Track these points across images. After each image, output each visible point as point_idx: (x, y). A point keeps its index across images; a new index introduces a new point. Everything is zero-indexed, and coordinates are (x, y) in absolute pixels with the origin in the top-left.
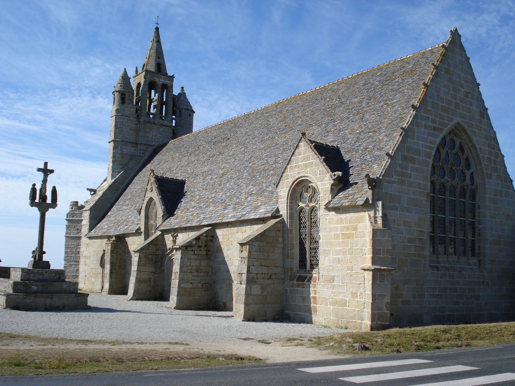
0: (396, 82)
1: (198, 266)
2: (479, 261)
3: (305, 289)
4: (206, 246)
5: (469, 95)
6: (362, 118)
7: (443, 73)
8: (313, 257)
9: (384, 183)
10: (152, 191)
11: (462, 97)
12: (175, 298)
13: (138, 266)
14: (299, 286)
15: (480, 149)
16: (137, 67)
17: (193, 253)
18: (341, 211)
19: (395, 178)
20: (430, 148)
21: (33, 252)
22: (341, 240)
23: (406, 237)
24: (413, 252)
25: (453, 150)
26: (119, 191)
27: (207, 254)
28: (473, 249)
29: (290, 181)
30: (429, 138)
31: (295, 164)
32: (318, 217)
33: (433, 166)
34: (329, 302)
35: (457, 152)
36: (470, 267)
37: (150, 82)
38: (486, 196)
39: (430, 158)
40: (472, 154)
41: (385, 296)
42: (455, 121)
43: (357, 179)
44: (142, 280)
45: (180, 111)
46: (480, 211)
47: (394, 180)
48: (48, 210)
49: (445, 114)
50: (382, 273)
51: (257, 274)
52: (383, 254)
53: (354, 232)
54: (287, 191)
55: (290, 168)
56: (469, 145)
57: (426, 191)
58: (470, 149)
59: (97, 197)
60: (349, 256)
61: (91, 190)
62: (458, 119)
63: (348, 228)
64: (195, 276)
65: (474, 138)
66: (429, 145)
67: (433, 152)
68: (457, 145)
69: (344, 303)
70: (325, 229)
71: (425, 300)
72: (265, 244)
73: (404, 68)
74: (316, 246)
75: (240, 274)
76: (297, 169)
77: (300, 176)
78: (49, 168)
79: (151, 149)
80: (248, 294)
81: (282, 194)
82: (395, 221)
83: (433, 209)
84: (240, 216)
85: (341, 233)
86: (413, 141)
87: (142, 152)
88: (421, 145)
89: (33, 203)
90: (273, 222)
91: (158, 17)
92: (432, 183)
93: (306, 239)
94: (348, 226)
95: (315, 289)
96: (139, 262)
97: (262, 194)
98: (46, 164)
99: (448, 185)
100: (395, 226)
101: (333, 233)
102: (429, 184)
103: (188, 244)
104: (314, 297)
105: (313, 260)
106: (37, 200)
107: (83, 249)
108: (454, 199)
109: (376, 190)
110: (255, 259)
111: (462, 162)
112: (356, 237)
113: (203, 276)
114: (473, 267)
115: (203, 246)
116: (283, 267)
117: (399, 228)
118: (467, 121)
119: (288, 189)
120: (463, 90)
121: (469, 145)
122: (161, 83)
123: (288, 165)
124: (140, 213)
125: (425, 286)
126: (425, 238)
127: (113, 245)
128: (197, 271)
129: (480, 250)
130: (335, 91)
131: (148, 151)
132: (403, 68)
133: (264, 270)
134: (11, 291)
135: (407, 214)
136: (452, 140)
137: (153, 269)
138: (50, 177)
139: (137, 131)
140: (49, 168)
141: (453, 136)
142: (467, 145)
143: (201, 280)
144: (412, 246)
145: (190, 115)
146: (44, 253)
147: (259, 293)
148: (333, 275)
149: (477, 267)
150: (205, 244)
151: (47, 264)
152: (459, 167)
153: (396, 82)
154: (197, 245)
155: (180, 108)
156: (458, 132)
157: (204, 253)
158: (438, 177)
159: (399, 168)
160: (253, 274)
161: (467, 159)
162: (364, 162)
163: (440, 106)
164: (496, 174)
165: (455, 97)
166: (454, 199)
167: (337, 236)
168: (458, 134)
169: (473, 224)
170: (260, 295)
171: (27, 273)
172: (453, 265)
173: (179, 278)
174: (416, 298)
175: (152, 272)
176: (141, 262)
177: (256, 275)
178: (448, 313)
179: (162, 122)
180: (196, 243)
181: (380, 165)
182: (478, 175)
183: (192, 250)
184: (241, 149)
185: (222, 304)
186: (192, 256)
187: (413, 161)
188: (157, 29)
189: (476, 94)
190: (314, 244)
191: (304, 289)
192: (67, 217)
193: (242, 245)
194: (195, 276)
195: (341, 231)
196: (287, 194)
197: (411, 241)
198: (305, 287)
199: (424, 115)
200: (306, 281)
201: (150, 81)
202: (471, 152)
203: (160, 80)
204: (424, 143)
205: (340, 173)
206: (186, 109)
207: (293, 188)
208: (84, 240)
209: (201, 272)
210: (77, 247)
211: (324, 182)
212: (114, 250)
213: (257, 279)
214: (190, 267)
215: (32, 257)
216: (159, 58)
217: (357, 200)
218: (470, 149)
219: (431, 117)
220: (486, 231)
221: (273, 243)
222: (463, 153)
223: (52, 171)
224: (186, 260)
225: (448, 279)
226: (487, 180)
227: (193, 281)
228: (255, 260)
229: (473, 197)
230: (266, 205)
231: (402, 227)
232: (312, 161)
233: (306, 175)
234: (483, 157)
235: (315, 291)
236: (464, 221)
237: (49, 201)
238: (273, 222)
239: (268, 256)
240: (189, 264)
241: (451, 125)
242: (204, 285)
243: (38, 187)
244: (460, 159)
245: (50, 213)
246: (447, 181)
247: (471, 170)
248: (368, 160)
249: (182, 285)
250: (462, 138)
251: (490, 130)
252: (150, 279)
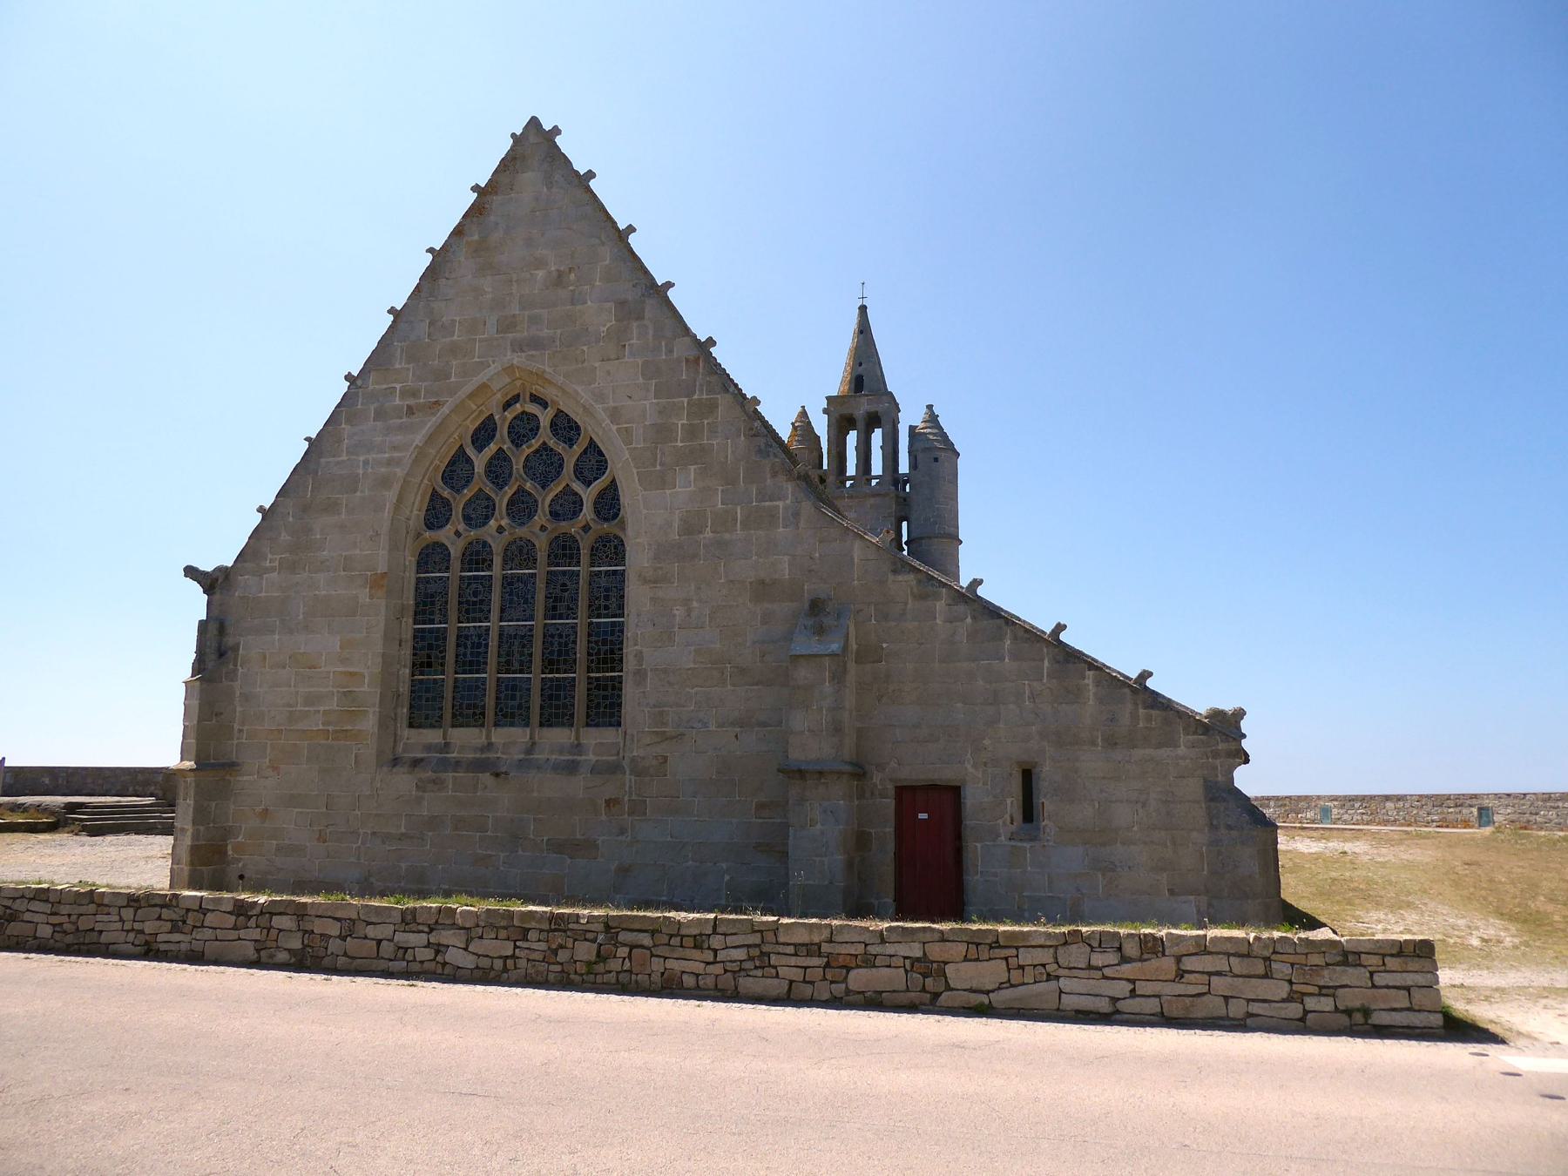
23: (297, 692)
24: (321, 727)
126: (366, 688)
187: (331, 507)
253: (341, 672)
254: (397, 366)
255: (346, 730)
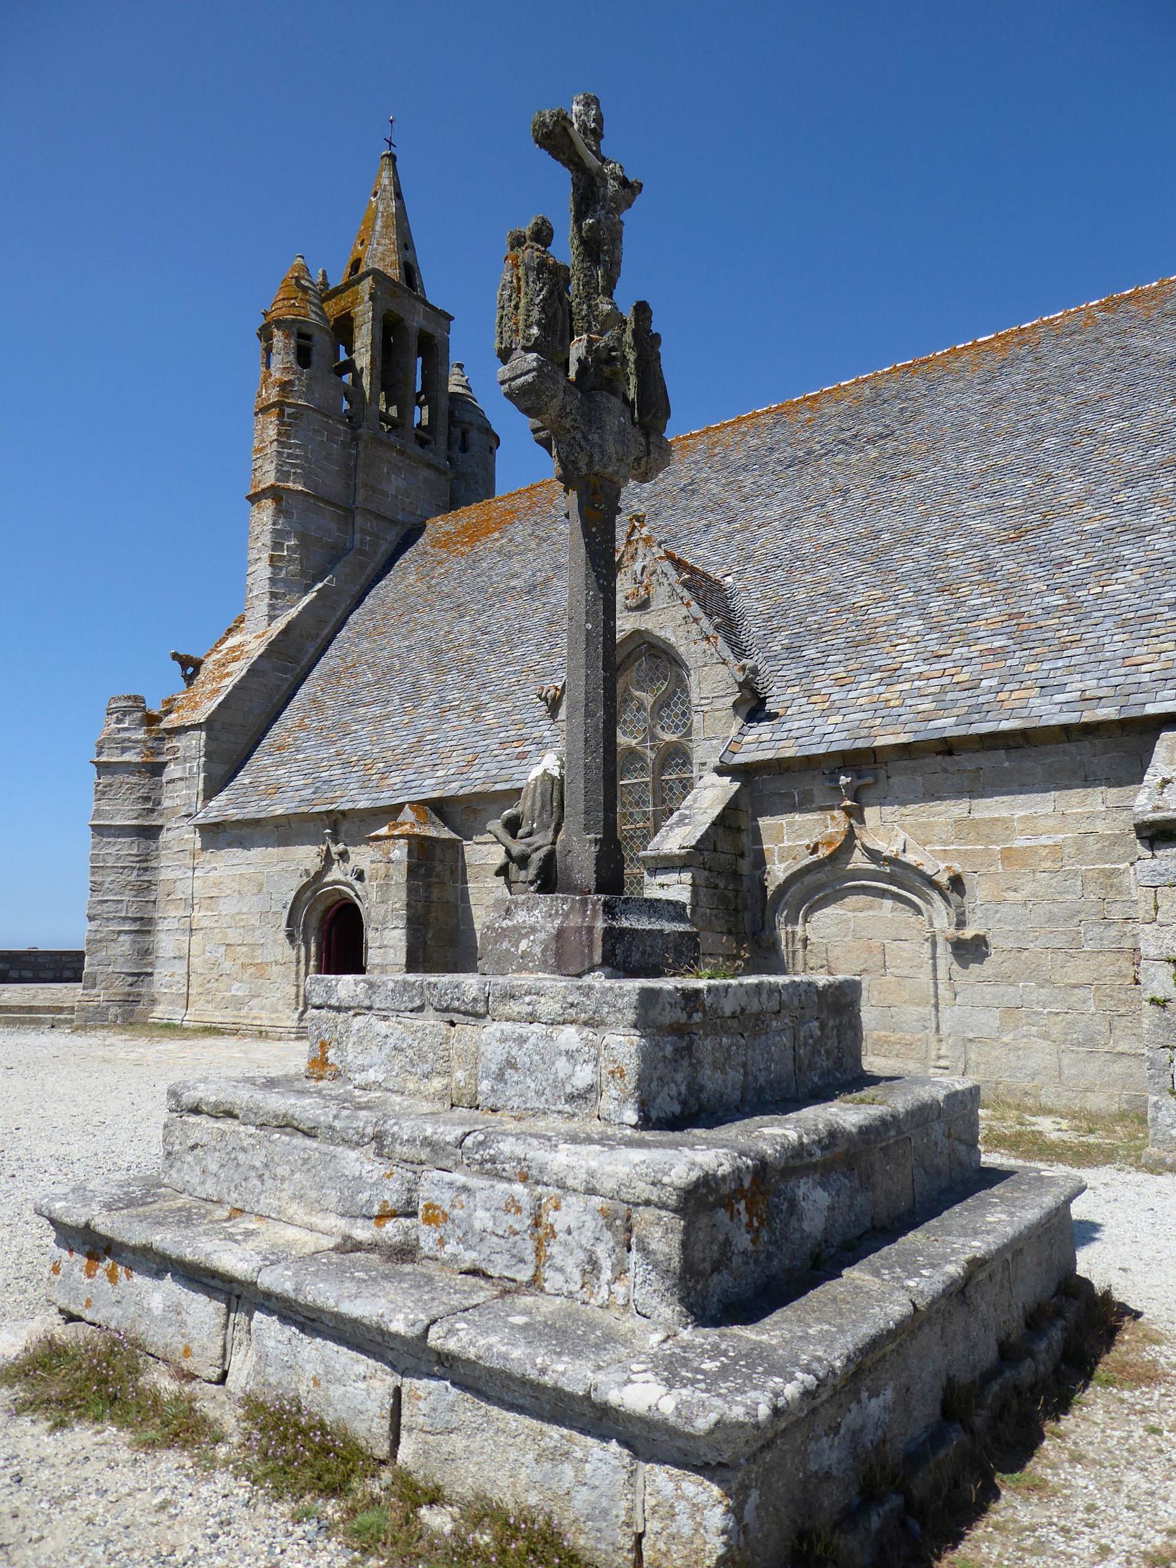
45: (464, 434)
79: (392, 536)
127: (414, 842)
139: (350, 471)
210: (145, 865)
212: (419, 866)
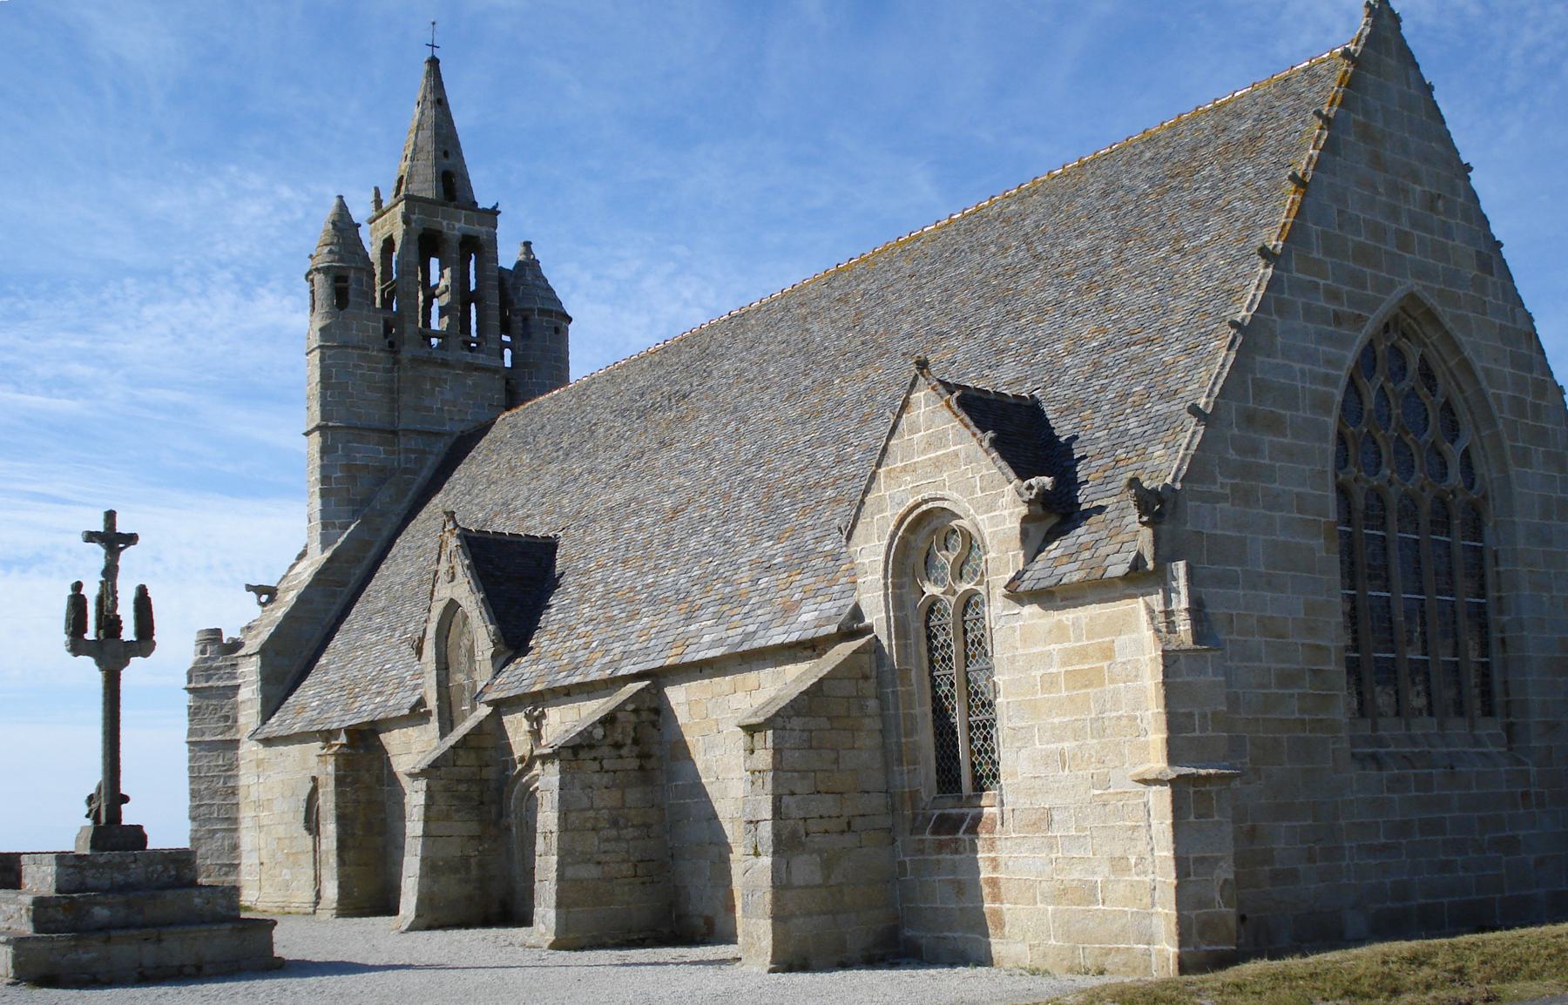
0: (1205, 179)
1: (615, 808)
2: (1509, 728)
3: (963, 856)
4: (636, 742)
5: (1440, 203)
6: (1104, 301)
7: (1352, 139)
8: (979, 752)
9: (1189, 503)
10: (452, 581)
11: (1418, 210)
12: (551, 915)
13: (427, 821)
14: (941, 847)
15: (1486, 371)
16: (377, 190)
17: (596, 766)
18: (1059, 599)
19: (1221, 484)
20: (1327, 380)
21: (90, 799)
22: (1064, 694)
23: (1269, 669)
24: (1297, 715)
25: (1400, 381)
26: (350, 586)
27: (641, 768)
28: (1487, 693)
29: (891, 515)
30: (1321, 348)
31: (902, 461)
32: (987, 626)
33: (1341, 439)
34: (1042, 894)
35: (1413, 389)
36: (1480, 750)
37: (421, 231)
38: (1517, 519)
39: (1328, 412)
40: (1462, 391)
41: (1217, 860)
42: (1399, 292)
43: (1102, 495)
44: (441, 863)
45: (525, 319)
46: (1501, 569)
47: (1220, 491)
48: (127, 663)
49: (1369, 271)
50: (1203, 789)
51: (805, 819)
52: (1203, 729)
53: (1105, 664)
54: (883, 550)
55: (885, 477)
56: (1452, 363)
57: (1323, 520)
58: (1453, 376)
59: (279, 612)
60: (1095, 741)
61: (259, 590)
62: (1408, 284)
63: (1083, 654)
64: (607, 840)
65: (1464, 339)
66: (1323, 370)
67: (1338, 395)
68: (1413, 364)
69: (1088, 893)
70: (1012, 660)
71: (1344, 864)
72: (823, 722)
73: (1226, 133)
74: (987, 716)
75: (751, 822)
76: (909, 478)
77: (919, 498)
78: (122, 527)
79: (441, 447)
80: (781, 885)
81: (867, 561)
82: (1232, 621)
83: (1350, 574)
84: (738, 639)
85: (1063, 670)
86: (1272, 360)
87: (413, 456)
88: (1299, 375)
89: (77, 645)
90: (844, 649)
91: (434, 23)
92: (1342, 491)
93: (953, 696)
94: (1084, 648)
95: (992, 855)
96: (427, 807)
97: (805, 565)
98: (110, 516)
99: (1393, 496)
100: (1232, 637)
101: (1039, 673)
102: (1332, 495)
103: (578, 741)
104: (992, 878)
105: (980, 764)
106: (90, 635)
107: (247, 778)
108: (1415, 537)
109: (1165, 527)
110: (795, 771)
111: (1431, 418)
112: (1112, 681)
113: (634, 839)
114: (1491, 749)
115: (629, 741)
116: (887, 792)
117: (1245, 641)
118: (1437, 287)
119: (886, 542)
120: (1418, 188)
121: (1452, 363)
122: (456, 232)
123: (879, 465)
124: (419, 651)
125: (1342, 822)
126: (1332, 667)
127: (340, 759)
128: (615, 823)
129: (1507, 694)
130: (1014, 220)
131: (431, 453)
132: (1223, 131)
133: (827, 805)
134: (27, 929)
135: (1269, 595)
136: (1397, 352)
137: (474, 827)
138: (127, 557)
139: (392, 394)
140: (122, 527)
141: (1399, 339)
142: (1445, 362)
143: (628, 852)
144: (1292, 696)
145: (557, 330)
146: (126, 799)
147: (818, 879)
148: (1047, 806)
149: (1505, 749)
150: (632, 734)
151: (137, 836)
152: (1422, 435)
153: (1205, 179)
154: (609, 740)
155: (523, 310)
156: (1412, 322)
157: (634, 764)
158: (1359, 471)
159: (1231, 451)
160: (792, 822)
161: (1448, 408)
162: (1119, 440)
163: (1350, 244)
164: (1541, 449)
165: (1394, 213)
166: (1415, 537)
167: (1050, 682)
168: (1415, 331)
169: (1479, 613)
170: (819, 886)
171: (74, 866)
172: (1427, 749)
173: (559, 848)
174: (1314, 862)
175: (472, 837)
176: (434, 809)
177: (801, 823)
178: (1422, 901)
179: (469, 357)
180: (605, 736)
181: (1170, 445)
182: (1485, 456)
183: (595, 759)
184: (726, 425)
185: (700, 922)
186: (596, 777)
187: (1274, 424)
188: (434, 63)
189: (1461, 200)
190: (980, 712)
191: (957, 857)
192: (190, 681)
193: (751, 730)
194: (607, 840)
195: (1064, 664)
196: (882, 558)
197: (1287, 679)
198: (961, 849)
199: (1301, 276)
200: (962, 831)
201: (424, 229)
202: (1458, 384)
203: (455, 226)
204: (1307, 367)
205: (1047, 481)
206: (542, 312)
207: (902, 538)
208: (249, 750)
209: (626, 827)
210: (229, 773)
211: (997, 513)
212: (345, 776)
213: (807, 834)
214: (591, 813)
215: (87, 816)
216: (446, 154)
217: (1106, 563)
218: (1453, 376)
219: (1322, 282)
220: (1525, 633)
221: (848, 716)
222: (1432, 389)
223: (131, 539)
224: (577, 791)
225: (1414, 793)
226: (1514, 470)
227: (603, 858)
228: (795, 774)
229: (1476, 527)
230: (819, 599)
231: (1257, 638)
232: (955, 448)
233: (940, 494)
234: (1498, 397)
235: (994, 859)
236: (1452, 606)
237: (128, 633)
238: (844, 649)
239: (836, 761)
240: (585, 802)
241: (1388, 304)
242: (641, 865)
243: (91, 592)
244: (1426, 410)
245: (134, 673)
246: (1389, 481)
247: (1462, 443)
248: (1131, 432)
249: (570, 872)
250: (1428, 341)
251: (1512, 310)
252: (465, 859)
253: (1310, 646)
254: (1315, 255)
255: (1321, 720)
